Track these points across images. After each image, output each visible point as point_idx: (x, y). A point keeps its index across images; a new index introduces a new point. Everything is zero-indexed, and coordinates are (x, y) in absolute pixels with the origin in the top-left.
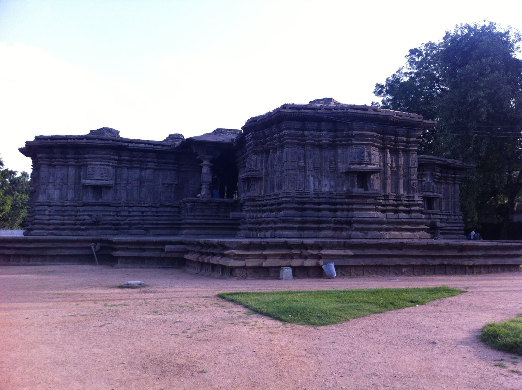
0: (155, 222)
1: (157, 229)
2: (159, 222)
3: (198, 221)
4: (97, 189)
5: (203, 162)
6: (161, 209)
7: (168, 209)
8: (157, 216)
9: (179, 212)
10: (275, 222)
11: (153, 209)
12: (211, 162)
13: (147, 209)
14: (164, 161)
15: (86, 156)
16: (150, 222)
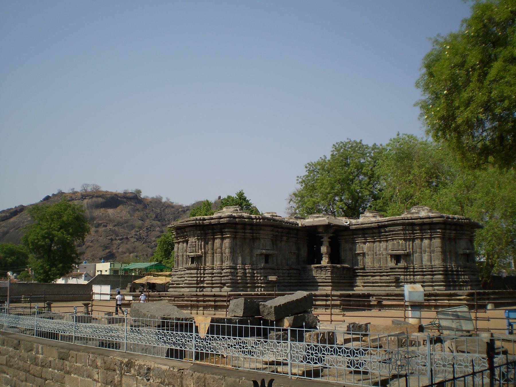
0: (290, 281)
1: (290, 286)
2: (292, 281)
3: (336, 281)
4: (267, 258)
5: (322, 238)
6: (291, 271)
7: (295, 271)
8: (289, 276)
9: (300, 274)
10: (432, 282)
11: (287, 272)
12: (329, 238)
13: (284, 271)
14: (291, 235)
15: (261, 232)
16: (286, 281)
